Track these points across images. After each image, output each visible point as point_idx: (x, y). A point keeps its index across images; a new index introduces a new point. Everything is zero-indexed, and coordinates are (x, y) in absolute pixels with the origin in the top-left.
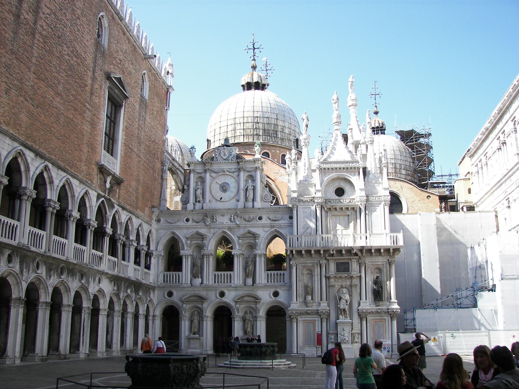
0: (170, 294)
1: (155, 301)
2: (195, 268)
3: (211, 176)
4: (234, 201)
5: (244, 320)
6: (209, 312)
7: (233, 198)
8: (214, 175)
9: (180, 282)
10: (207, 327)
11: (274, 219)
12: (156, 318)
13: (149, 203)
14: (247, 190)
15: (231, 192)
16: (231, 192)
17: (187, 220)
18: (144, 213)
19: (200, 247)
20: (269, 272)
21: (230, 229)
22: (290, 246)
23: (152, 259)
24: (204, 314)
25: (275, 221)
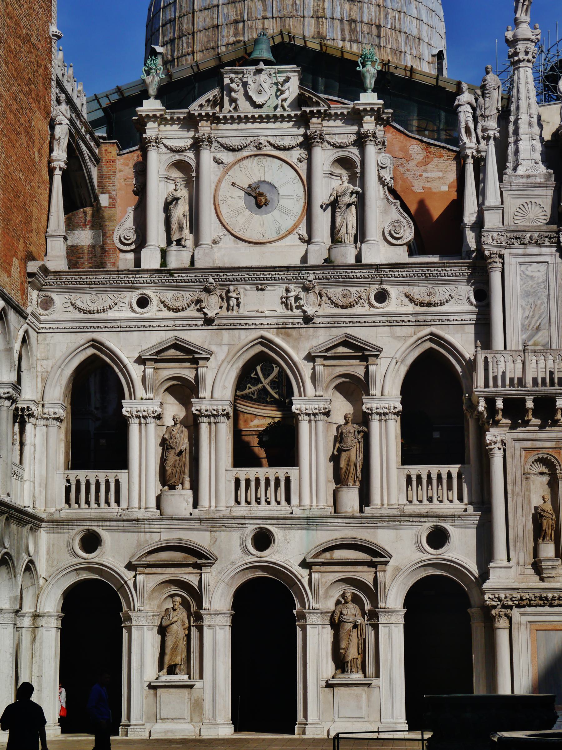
0: (91, 542)
1: (42, 567)
2: (172, 457)
3: (218, 161)
4: (293, 240)
5: (336, 624)
6: (219, 599)
7: (289, 233)
8: (227, 157)
9: (124, 504)
10: (215, 650)
11: (427, 299)
12: (42, 622)
13: (21, 246)
14: (334, 205)
15: (285, 212)
16: (285, 212)
17: (143, 302)
18: (10, 275)
19: (184, 391)
20: (414, 470)
21: (282, 328)
22: (487, 385)
23: (29, 427)
24: (205, 605)
25: (429, 305)
